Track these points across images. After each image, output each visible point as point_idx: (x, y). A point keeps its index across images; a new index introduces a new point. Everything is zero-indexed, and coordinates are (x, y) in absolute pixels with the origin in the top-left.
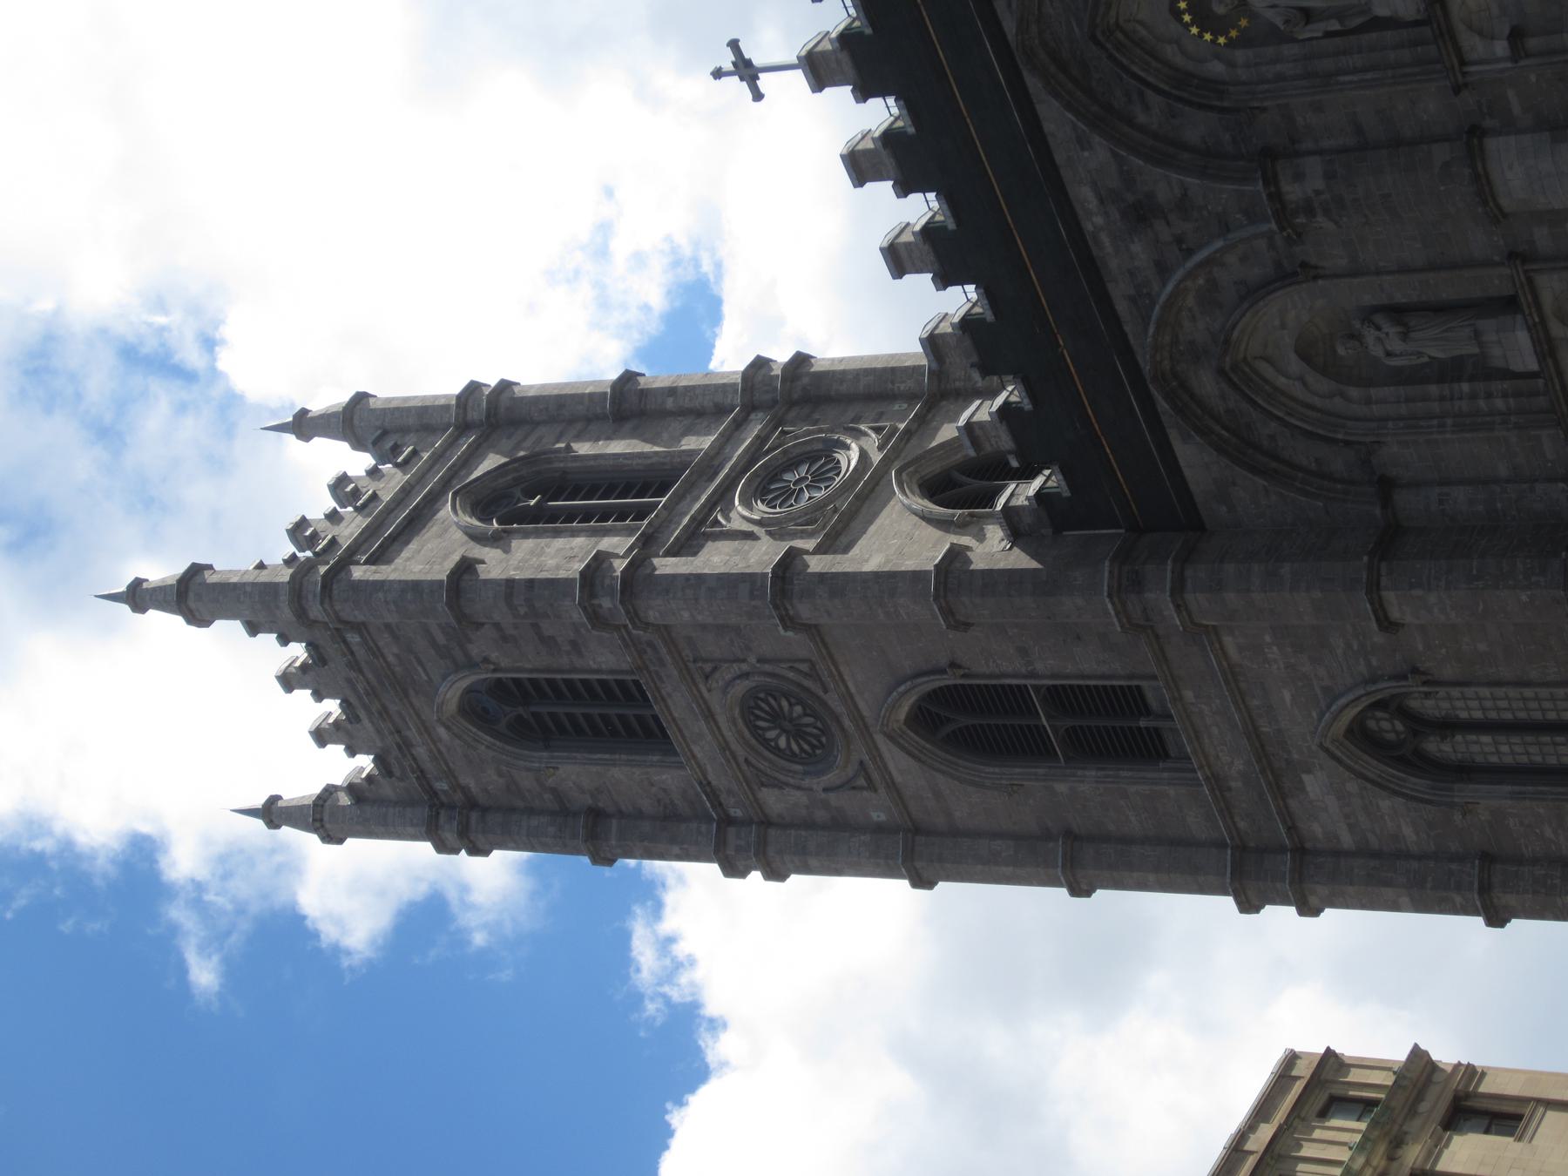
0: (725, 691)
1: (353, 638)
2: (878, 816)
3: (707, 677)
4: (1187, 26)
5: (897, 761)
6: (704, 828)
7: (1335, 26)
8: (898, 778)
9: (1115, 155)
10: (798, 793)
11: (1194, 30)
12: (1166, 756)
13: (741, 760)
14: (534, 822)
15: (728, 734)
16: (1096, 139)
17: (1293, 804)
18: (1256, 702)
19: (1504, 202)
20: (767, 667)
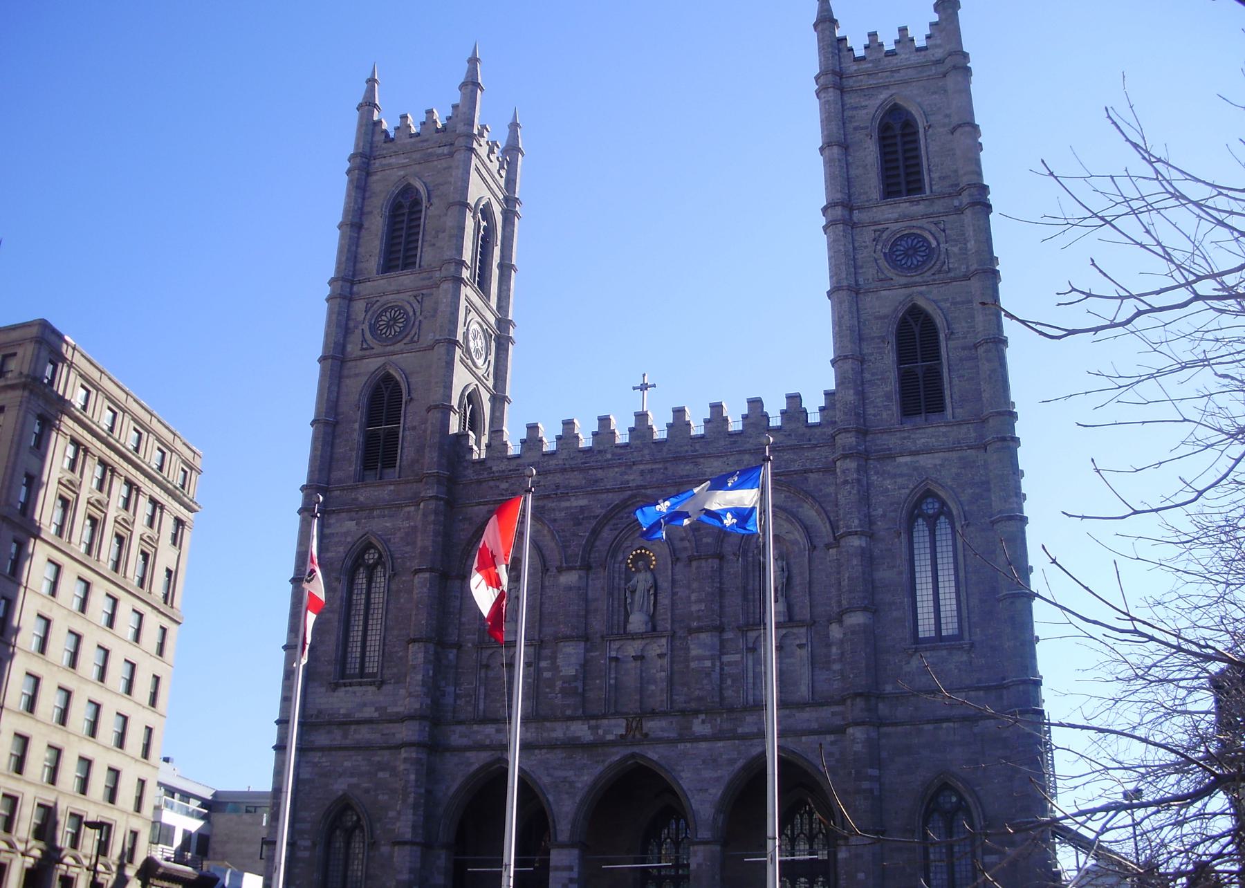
0: (408, 302)
1: (446, 150)
2: (349, 348)
3: (415, 297)
4: (636, 551)
5: (373, 364)
6: (351, 273)
7: (629, 600)
8: (365, 361)
9: (598, 516)
10: (363, 317)
11: (634, 553)
12: (365, 469)
13: (378, 298)
14: (360, 200)
15: (390, 297)
16: (604, 511)
17: (344, 515)
18: (386, 512)
19: (562, 644)
20: (417, 323)
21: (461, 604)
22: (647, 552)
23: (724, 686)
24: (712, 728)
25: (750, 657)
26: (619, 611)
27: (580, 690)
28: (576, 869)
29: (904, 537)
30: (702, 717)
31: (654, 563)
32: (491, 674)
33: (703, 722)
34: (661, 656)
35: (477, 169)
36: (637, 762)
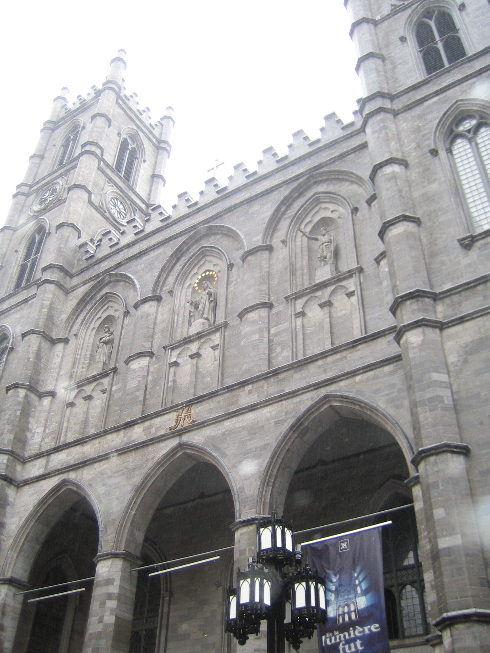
4: (202, 275)
11: (200, 277)
21: (62, 361)
22: (211, 273)
23: (274, 355)
24: (258, 396)
25: (299, 321)
26: (183, 325)
27: (141, 398)
28: (117, 583)
29: (442, 154)
30: (249, 388)
31: (216, 279)
32: (75, 410)
33: (250, 392)
34: (214, 348)
35: (117, 103)
36: (185, 453)
